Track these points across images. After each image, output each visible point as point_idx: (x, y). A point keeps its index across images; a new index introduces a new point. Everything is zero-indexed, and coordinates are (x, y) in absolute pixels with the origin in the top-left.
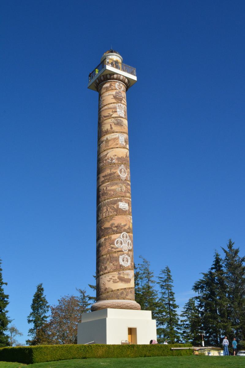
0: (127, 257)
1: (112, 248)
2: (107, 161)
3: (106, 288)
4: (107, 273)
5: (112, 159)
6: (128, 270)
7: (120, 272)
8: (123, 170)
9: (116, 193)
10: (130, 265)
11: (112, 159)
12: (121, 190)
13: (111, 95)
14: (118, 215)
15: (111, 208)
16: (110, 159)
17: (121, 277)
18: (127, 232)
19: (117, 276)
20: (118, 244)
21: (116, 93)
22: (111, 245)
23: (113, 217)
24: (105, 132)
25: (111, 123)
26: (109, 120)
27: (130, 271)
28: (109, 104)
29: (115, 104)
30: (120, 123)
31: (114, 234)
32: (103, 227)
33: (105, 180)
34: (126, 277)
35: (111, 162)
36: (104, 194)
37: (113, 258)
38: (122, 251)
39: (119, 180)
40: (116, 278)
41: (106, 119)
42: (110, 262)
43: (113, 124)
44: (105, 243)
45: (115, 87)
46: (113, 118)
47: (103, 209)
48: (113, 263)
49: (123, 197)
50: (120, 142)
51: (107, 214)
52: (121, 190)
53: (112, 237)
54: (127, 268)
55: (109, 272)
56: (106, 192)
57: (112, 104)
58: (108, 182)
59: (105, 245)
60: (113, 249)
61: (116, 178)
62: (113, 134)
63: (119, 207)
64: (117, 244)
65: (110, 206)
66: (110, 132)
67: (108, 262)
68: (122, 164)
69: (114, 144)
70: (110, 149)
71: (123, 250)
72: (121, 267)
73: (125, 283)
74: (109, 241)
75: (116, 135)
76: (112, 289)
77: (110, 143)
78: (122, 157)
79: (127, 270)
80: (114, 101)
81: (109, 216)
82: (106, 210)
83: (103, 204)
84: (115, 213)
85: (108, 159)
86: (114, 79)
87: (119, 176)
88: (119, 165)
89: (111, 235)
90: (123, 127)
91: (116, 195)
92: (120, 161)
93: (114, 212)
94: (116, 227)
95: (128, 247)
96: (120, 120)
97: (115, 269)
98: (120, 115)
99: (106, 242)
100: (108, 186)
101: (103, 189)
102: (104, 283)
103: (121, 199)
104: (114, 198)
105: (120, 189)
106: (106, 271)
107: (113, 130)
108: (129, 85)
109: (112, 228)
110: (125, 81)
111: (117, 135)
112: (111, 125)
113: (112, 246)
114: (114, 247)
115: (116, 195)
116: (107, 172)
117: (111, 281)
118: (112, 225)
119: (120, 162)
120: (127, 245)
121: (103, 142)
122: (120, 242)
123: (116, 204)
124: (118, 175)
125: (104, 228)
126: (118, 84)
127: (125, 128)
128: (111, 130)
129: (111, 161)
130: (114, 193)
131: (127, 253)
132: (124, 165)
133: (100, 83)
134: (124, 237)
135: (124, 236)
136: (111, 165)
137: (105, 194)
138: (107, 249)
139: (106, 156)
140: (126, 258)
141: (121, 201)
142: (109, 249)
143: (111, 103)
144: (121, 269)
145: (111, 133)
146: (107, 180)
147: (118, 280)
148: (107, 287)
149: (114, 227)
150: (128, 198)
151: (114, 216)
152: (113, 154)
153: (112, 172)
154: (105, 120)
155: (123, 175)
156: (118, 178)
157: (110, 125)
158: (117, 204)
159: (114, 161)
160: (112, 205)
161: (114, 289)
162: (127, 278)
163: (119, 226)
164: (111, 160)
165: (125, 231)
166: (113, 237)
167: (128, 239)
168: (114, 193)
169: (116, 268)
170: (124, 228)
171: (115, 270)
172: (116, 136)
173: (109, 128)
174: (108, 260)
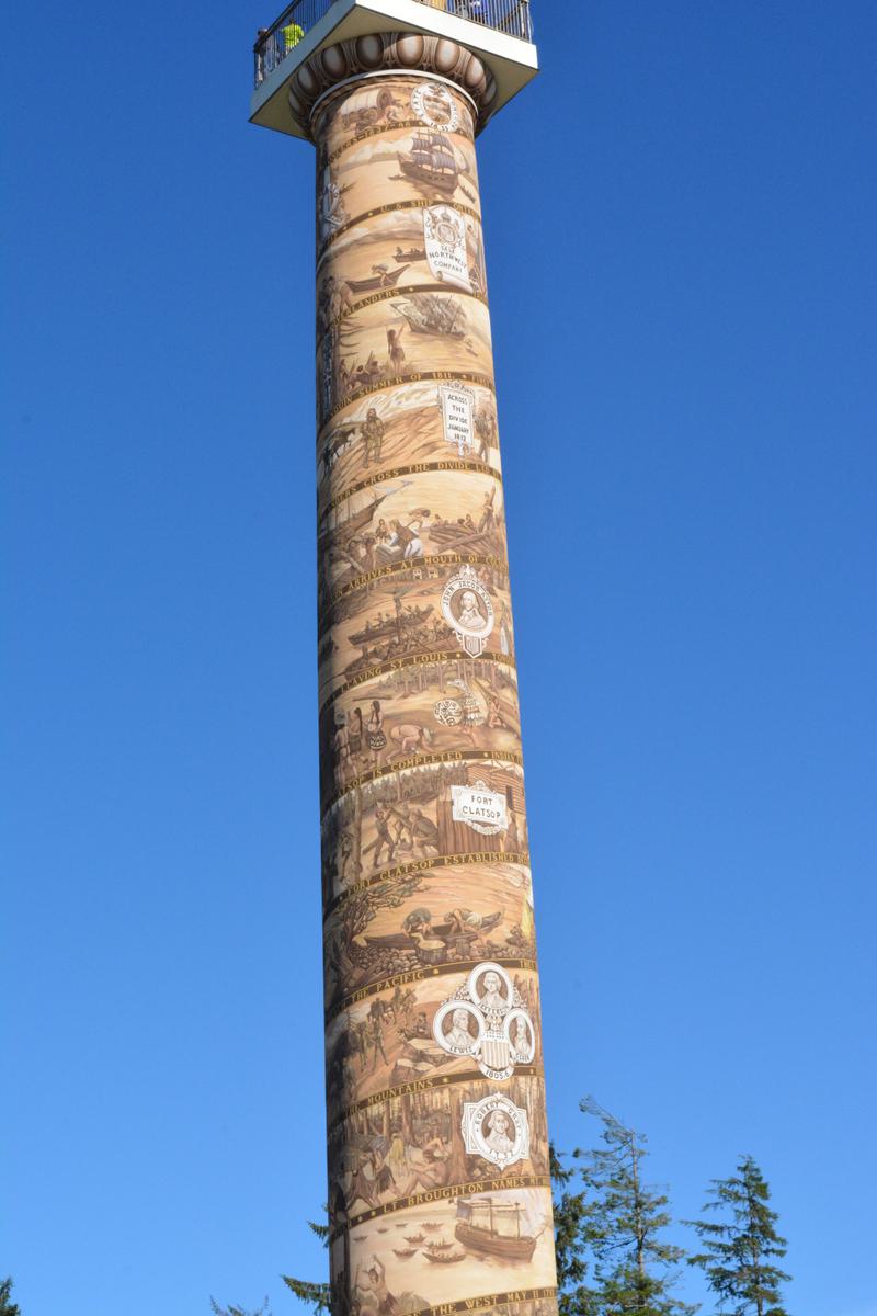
0: (506, 1109)
1: (421, 1056)
2: (375, 547)
3: (390, 1297)
4: (390, 1207)
5: (404, 537)
7: (467, 1202)
8: (469, 598)
9: (433, 735)
10: (526, 1156)
11: (404, 537)
12: (464, 712)
13: (386, 157)
14: (451, 861)
15: (404, 821)
16: (394, 535)
17: (477, 1228)
18: (506, 964)
19: (455, 1222)
20: (450, 1035)
21: (418, 145)
22: (410, 1038)
23: (421, 875)
24: (359, 378)
25: (396, 321)
26: (383, 308)
27: (525, 1191)
28: (377, 212)
29: (414, 213)
30: (445, 323)
31: (428, 974)
32: (363, 935)
33: (366, 657)
34: (505, 1228)
35: (401, 555)
37: (428, 1115)
38: (478, 1075)
39: (452, 656)
40: (447, 1233)
41: (364, 302)
42: (406, 1143)
43: (407, 329)
44: (376, 1028)
45: (411, 111)
46: (404, 291)
47: (359, 829)
48: (428, 1146)
49: (477, 754)
50: (451, 434)
51: (384, 858)
52: (464, 712)
53: (417, 994)
55: (402, 1204)
56: (372, 728)
57: (398, 213)
58: (385, 669)
59: (378, 1039)
60: (423, 1066)
61: (430, 647)
62: (405, 388)
63: (456, 818)
64: (446, 1032)
65: (399, 809)
66: (389, 377)
67: (397, 1143)
68: (465, 559)
69: (416, 443)
70: (392, 474)
71: (484, 1070)
72: (477, 1172)
73: (503, 1265)
74: (402, 1019)
75: (424, 392)
76: (427, 1303)
77: (391, 440)
78: (461, 521)
79: (507, 1187)
80: (406, 191)
81: (393, 872)
82: (375, 835)
83: (360, 805)
84: (432, 850)
85: (383, 534)
86: (401, 62)
87: (448, 632)
88: (446, 568)
89: (410, 979)
90: (462, 345)
91: (431, 745)
92: (452, 548)
93: (422, 845)
94: (441, 932)
95: (514, 1053)
96: (443, 301)
97: (439, 1180)
98: (446, 277)
99: (383, 1024)
101: (358, 711)
102: (379, 1270)
103: (465, 769)
104: (421, 763)
105: (454, 708)
106: (388, 1196)
107: (403, 364)
108: (489, 96)
109: (411, 942)
110: (466, 75)
111: (432, 394)
112: (391, 334)
113: (418, 1044)
114: (430, 1052)
115: (431, 745)
116: (377, 610)
117: (420, 1257)
118: (414, 922)
119: (450, 552)
120: (506, 1040)
121: (350, 437)
122: (464, 1024)
123: (437, 796)
124: (440, 627)
125: (368, 940)
126: (431, 95)
127: (475, 349)
128: (392, 364)
129: (397, 548)
130: (421, 732)
131: (506, 1085)
132: (478, 570)
133: (319, 88)
134: (487, 990)
135: (488, 986)
136: (398, 572)
137: (368, 741)
138: (392, 1066)
141: (466, 782)
142: (401, 1062)
143: (392, 207)
144: (473, 1179)
145: (394, 382)
146: (376, 661)
147: (458, 1248)
148: (396, 1294)
149: (427, 935)
150: (505, 764)
151: (424, 872)
152: (413, 508)
153: (407, 613)
154: (357, 307)
155: (472, 628)
156: (443, 648)
157: (386, 337)
158: (441, 798)
159: (416, 544)
160: (410, 806)
162: (513, 1232)
163: (459, 930)
165: (490, 953)
166: (426, 990)
167: (510, 1001)
168: (421, 732)
169: (447, 1177)
170: (485, 939)
171: (438, 1186)
172: (424, 398)
173: (382, 352)
174: (394, 1128)
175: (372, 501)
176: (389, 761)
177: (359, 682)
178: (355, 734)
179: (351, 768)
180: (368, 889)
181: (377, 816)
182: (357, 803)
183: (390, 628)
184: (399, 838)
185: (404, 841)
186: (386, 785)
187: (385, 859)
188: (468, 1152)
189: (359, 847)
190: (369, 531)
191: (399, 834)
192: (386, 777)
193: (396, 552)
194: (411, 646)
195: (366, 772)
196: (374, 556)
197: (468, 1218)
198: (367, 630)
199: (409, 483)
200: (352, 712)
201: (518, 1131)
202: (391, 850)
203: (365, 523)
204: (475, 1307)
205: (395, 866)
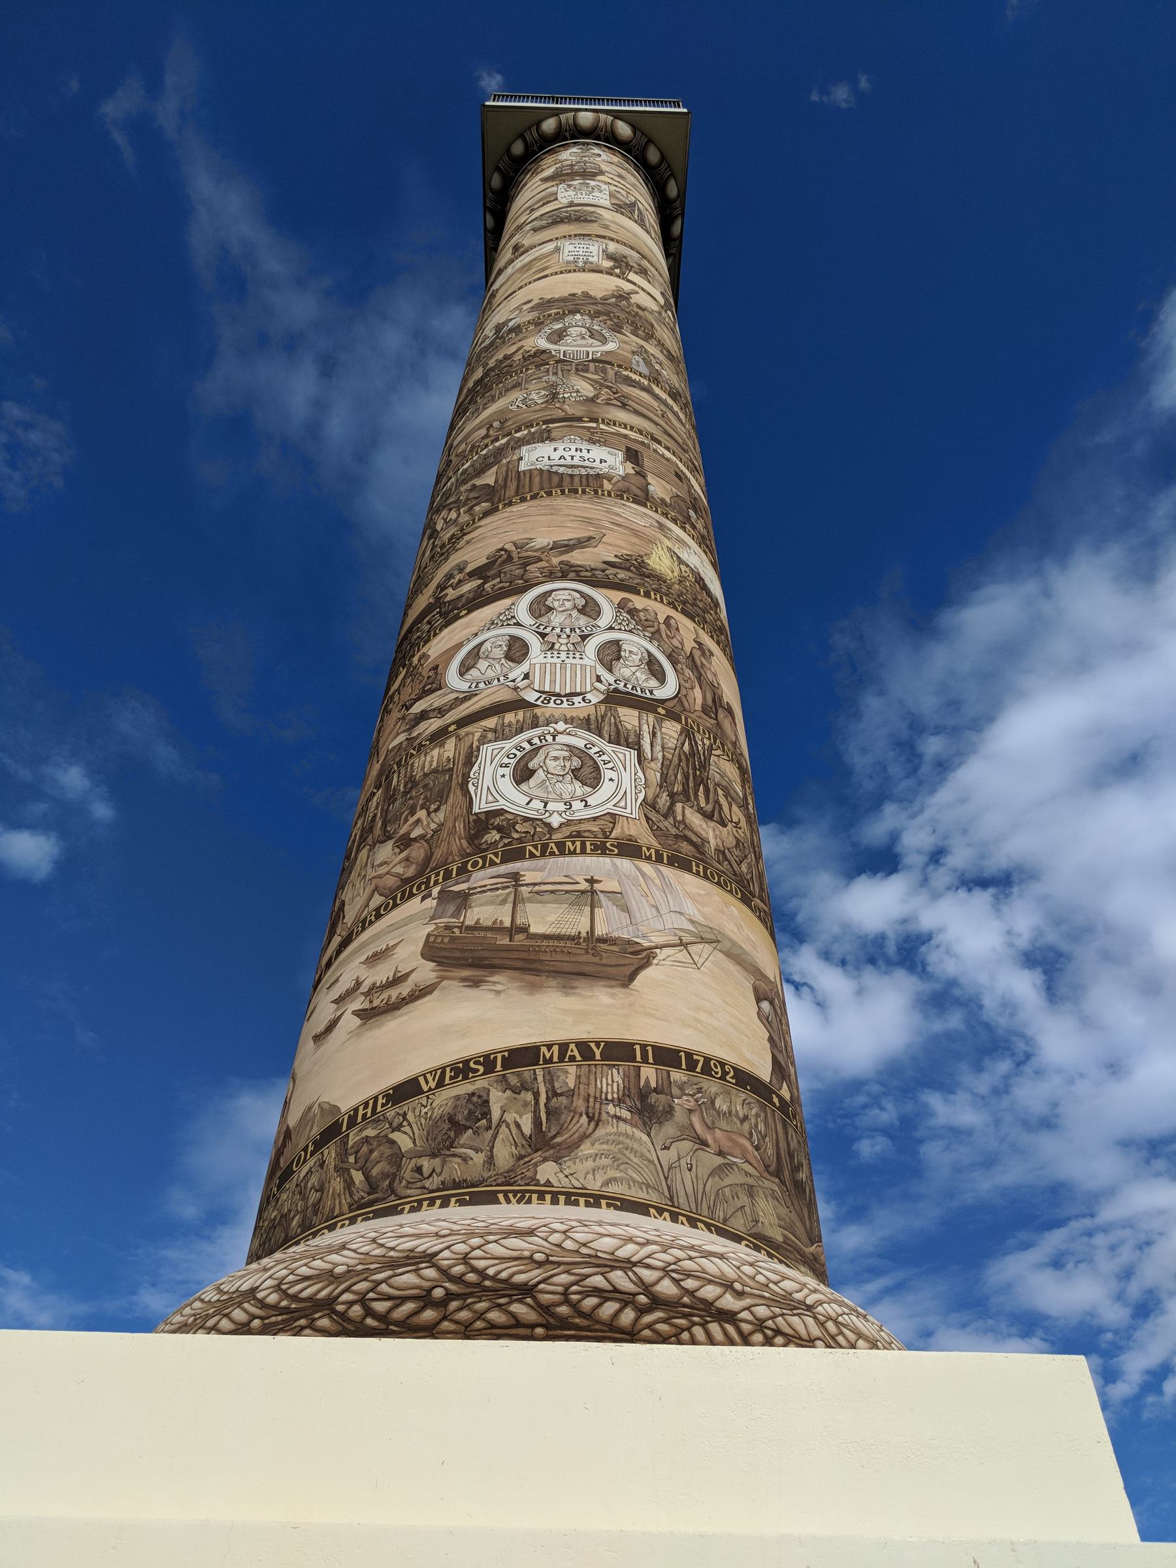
0: (580, 743)
6: (601, 849)
10: (632, 809)
27: (625, 864)
54: (579, 834)
79: (562, 850)
140: (571, 748)
161: (345, 1106)
188: (476, 810)
197: (456, 914)
201: (608, 774)
204: (441, 1084)
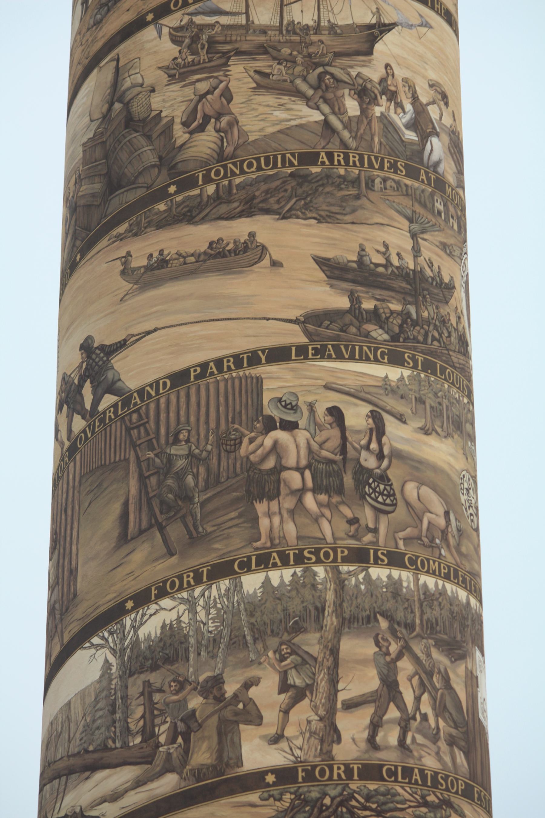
2: (378, 111)
36: (348, 480)
47: (334, 652)
51: (390, 736)
58: (396, 360)
65: (418, 648)
100: (391, 403)
101: (336, 413)
139: (370, 52)
164: (413, 125)
175: (369, 19)
176: (401, 543)
177: (340, 357)
178: (324, 453)
179: (316, 520)
180: (354, 786)
181: (377, 644)
182: (330, 596)
183: (404, 285)
184: (418, 708)
185: (425, 717)
186: (395, 587)
187: (393, 739)
189: (333, 690)
190: (366, 72)
191: (418, 699)
192: (395, 573)
193: (412, 143)
194: (434, 339)
195: (353, 543)
196: (376, 126)
198: (360, 262)
199: (426, 24)
200: (321, 410)
202: (405, 725)
203: (358, 53)
205: (411, 763)
